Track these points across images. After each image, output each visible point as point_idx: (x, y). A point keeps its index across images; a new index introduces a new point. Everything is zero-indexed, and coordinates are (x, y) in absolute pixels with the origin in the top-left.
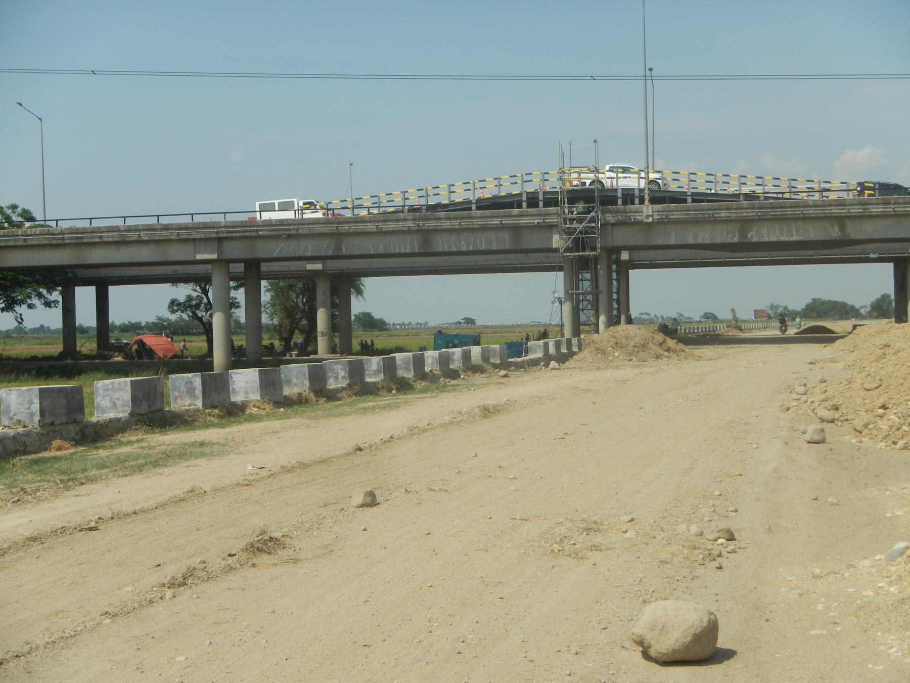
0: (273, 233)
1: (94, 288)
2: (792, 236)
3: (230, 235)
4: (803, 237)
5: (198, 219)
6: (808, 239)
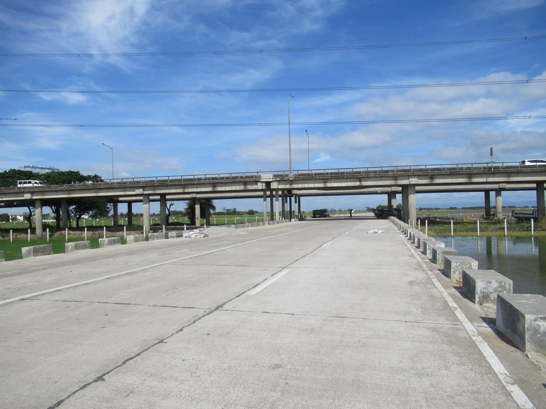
0: (161, 184)
1: (127, 203)
3: (146, 185)
5: (135, 180)
6: (348, 186)
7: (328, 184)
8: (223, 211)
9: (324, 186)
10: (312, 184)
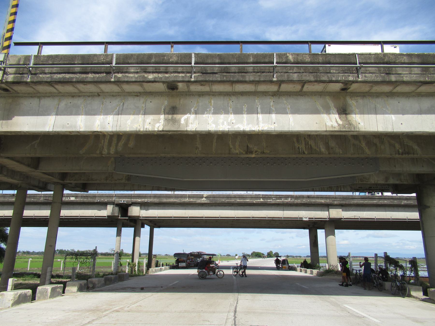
2: (258, 124)
4: (276, 125)
7: (187, 120)
8: (111, 252)
9: (167, 129)
10: (107, 113)
